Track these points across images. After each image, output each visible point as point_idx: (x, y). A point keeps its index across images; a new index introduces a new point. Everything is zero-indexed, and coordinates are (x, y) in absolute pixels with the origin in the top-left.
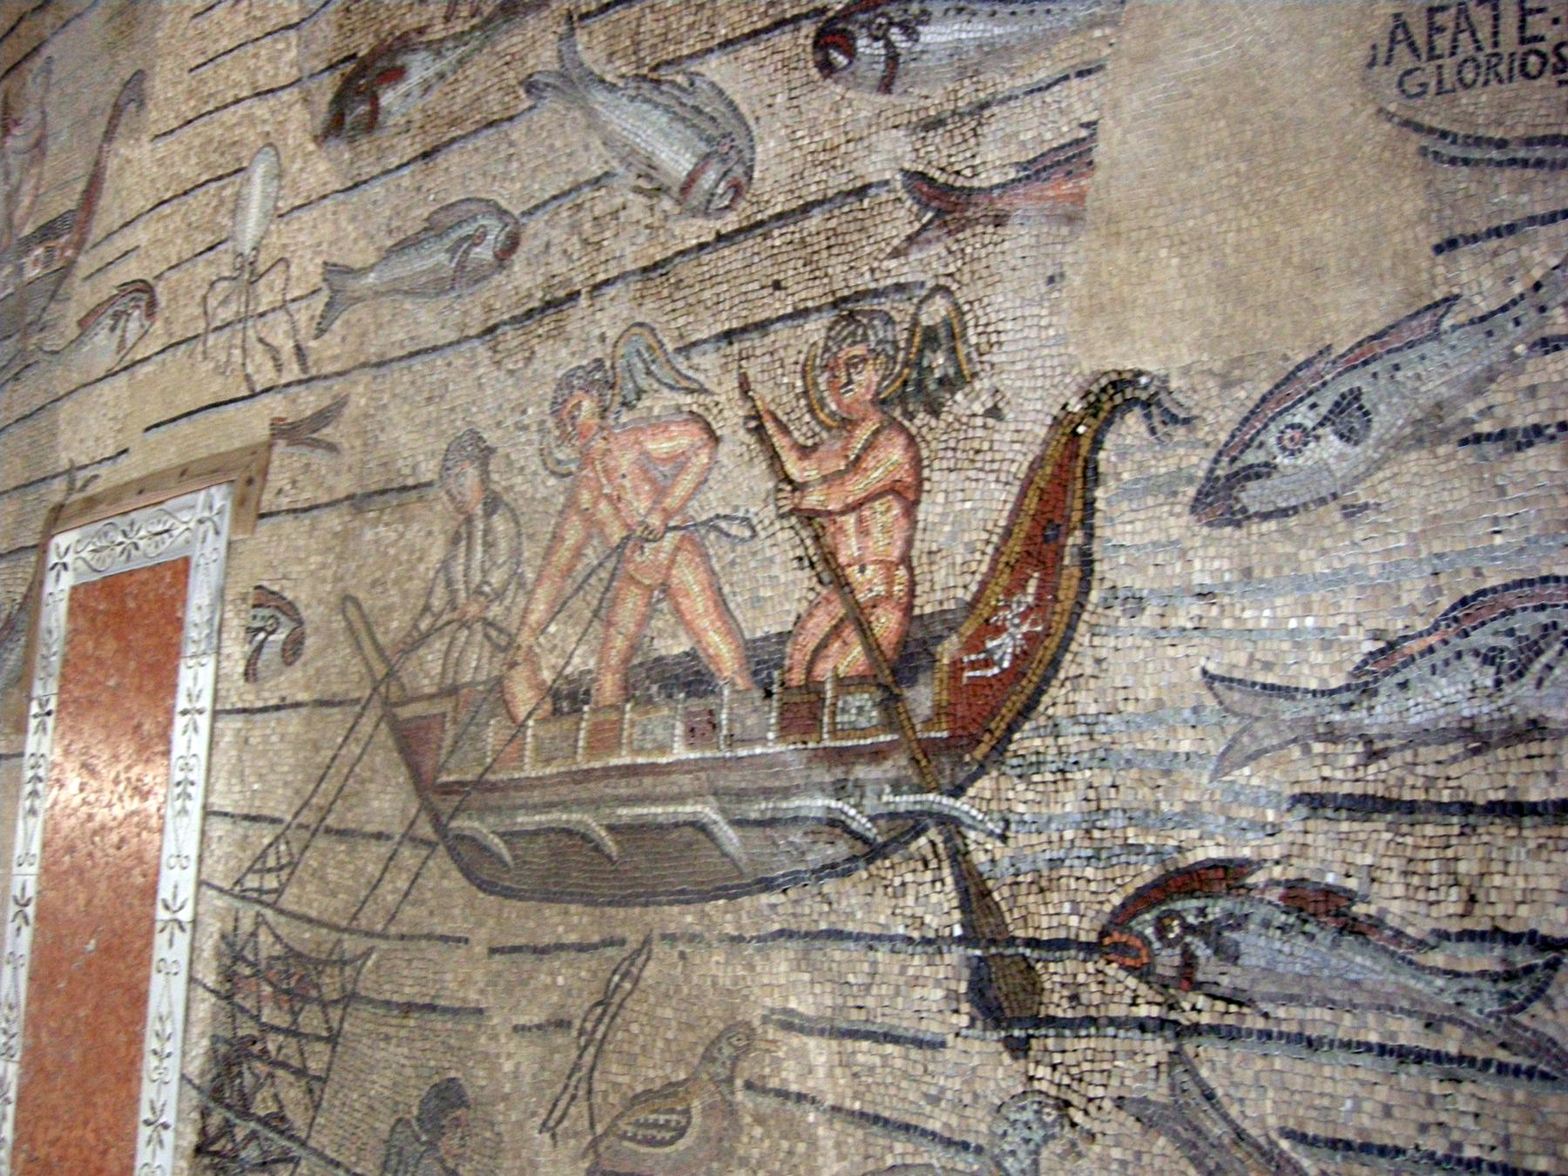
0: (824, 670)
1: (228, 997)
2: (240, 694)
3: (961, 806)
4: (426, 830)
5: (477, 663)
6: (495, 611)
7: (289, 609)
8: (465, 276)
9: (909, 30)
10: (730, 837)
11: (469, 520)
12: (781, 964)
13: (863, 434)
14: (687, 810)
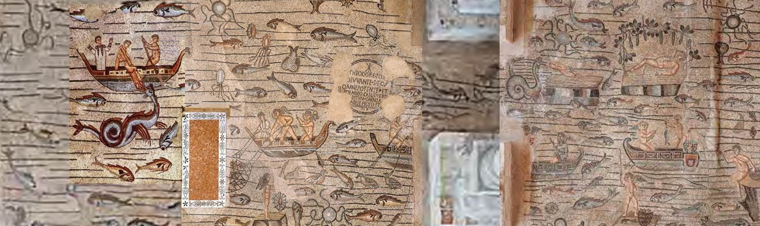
0: (305, 139)
1: (233, 168)
2: (230, 136)
3: (317, 150)
4: (260, 151)
5: (265, 135)
6: (267, 131)
7: (237, 128)
8: (259, 96)
9: (313, 87)
10: (296, 152)
11: (262, 121)
12: (302, 162)
13: (308, 121)
14: (292, 150)
